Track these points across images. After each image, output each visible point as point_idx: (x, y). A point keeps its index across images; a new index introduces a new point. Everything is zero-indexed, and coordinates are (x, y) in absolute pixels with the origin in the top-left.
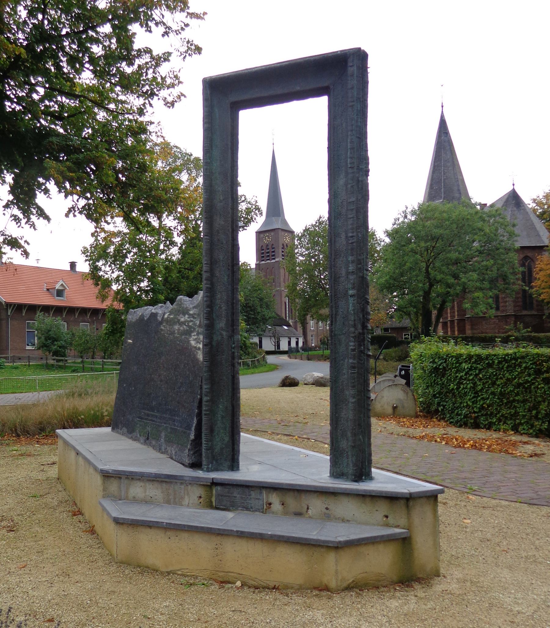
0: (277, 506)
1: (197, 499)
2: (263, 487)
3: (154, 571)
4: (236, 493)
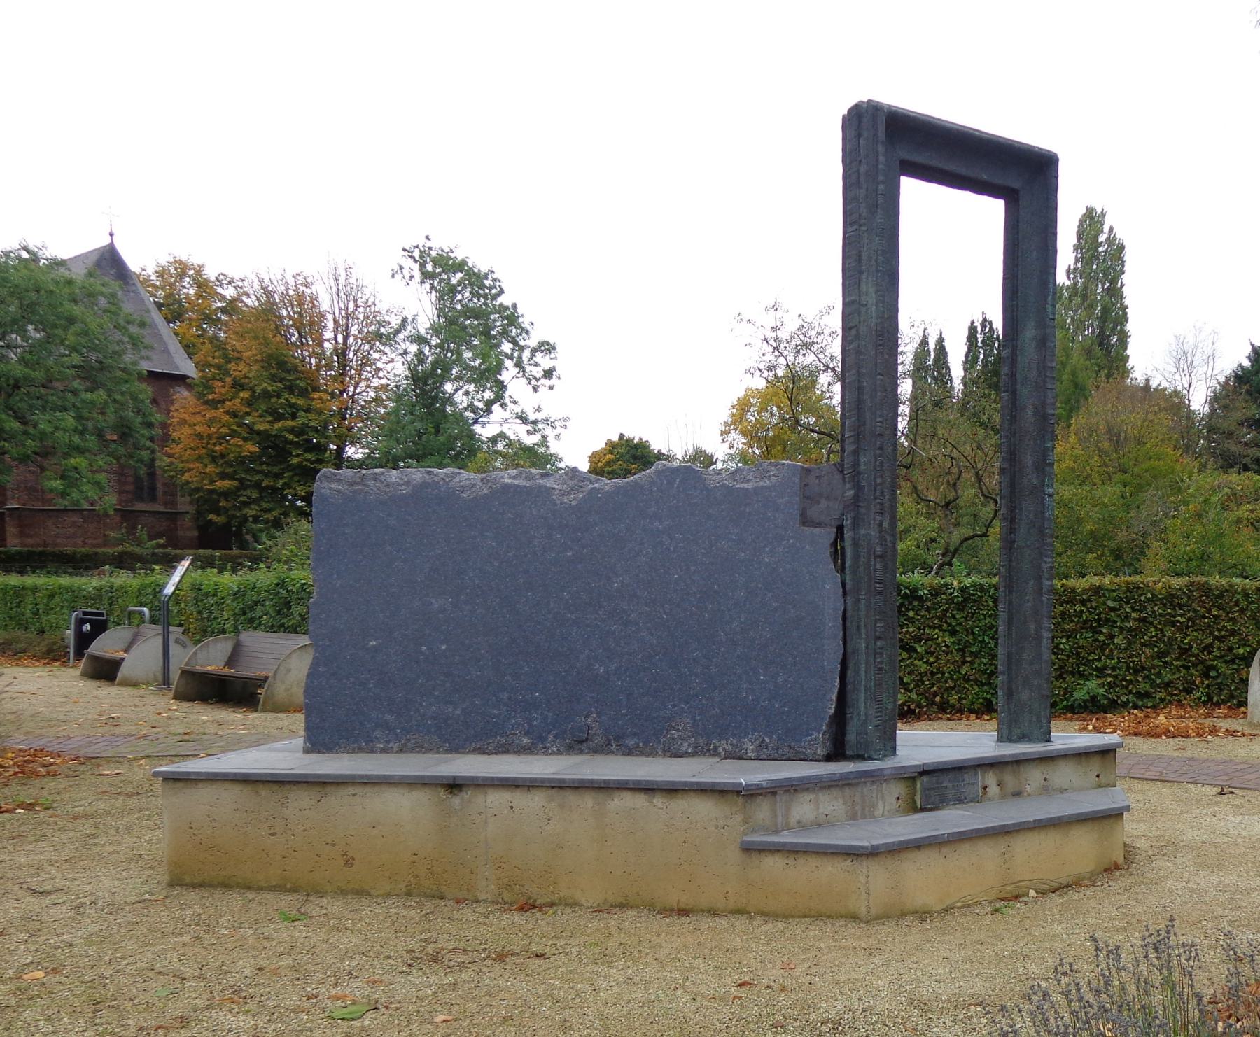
0: (993, 790)
1: (894, 801)
2: (979, 766)
3: (924, 914)
4: (947, 782)
